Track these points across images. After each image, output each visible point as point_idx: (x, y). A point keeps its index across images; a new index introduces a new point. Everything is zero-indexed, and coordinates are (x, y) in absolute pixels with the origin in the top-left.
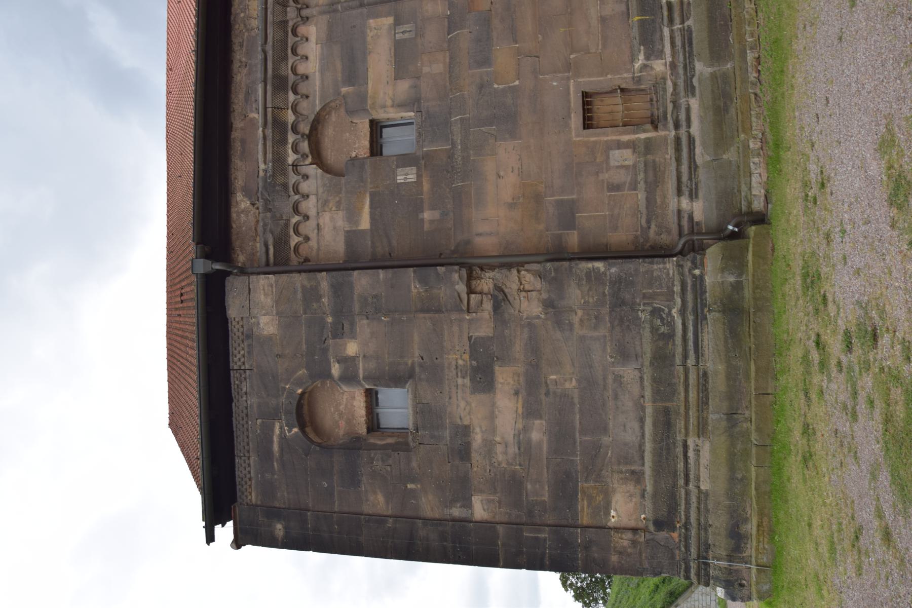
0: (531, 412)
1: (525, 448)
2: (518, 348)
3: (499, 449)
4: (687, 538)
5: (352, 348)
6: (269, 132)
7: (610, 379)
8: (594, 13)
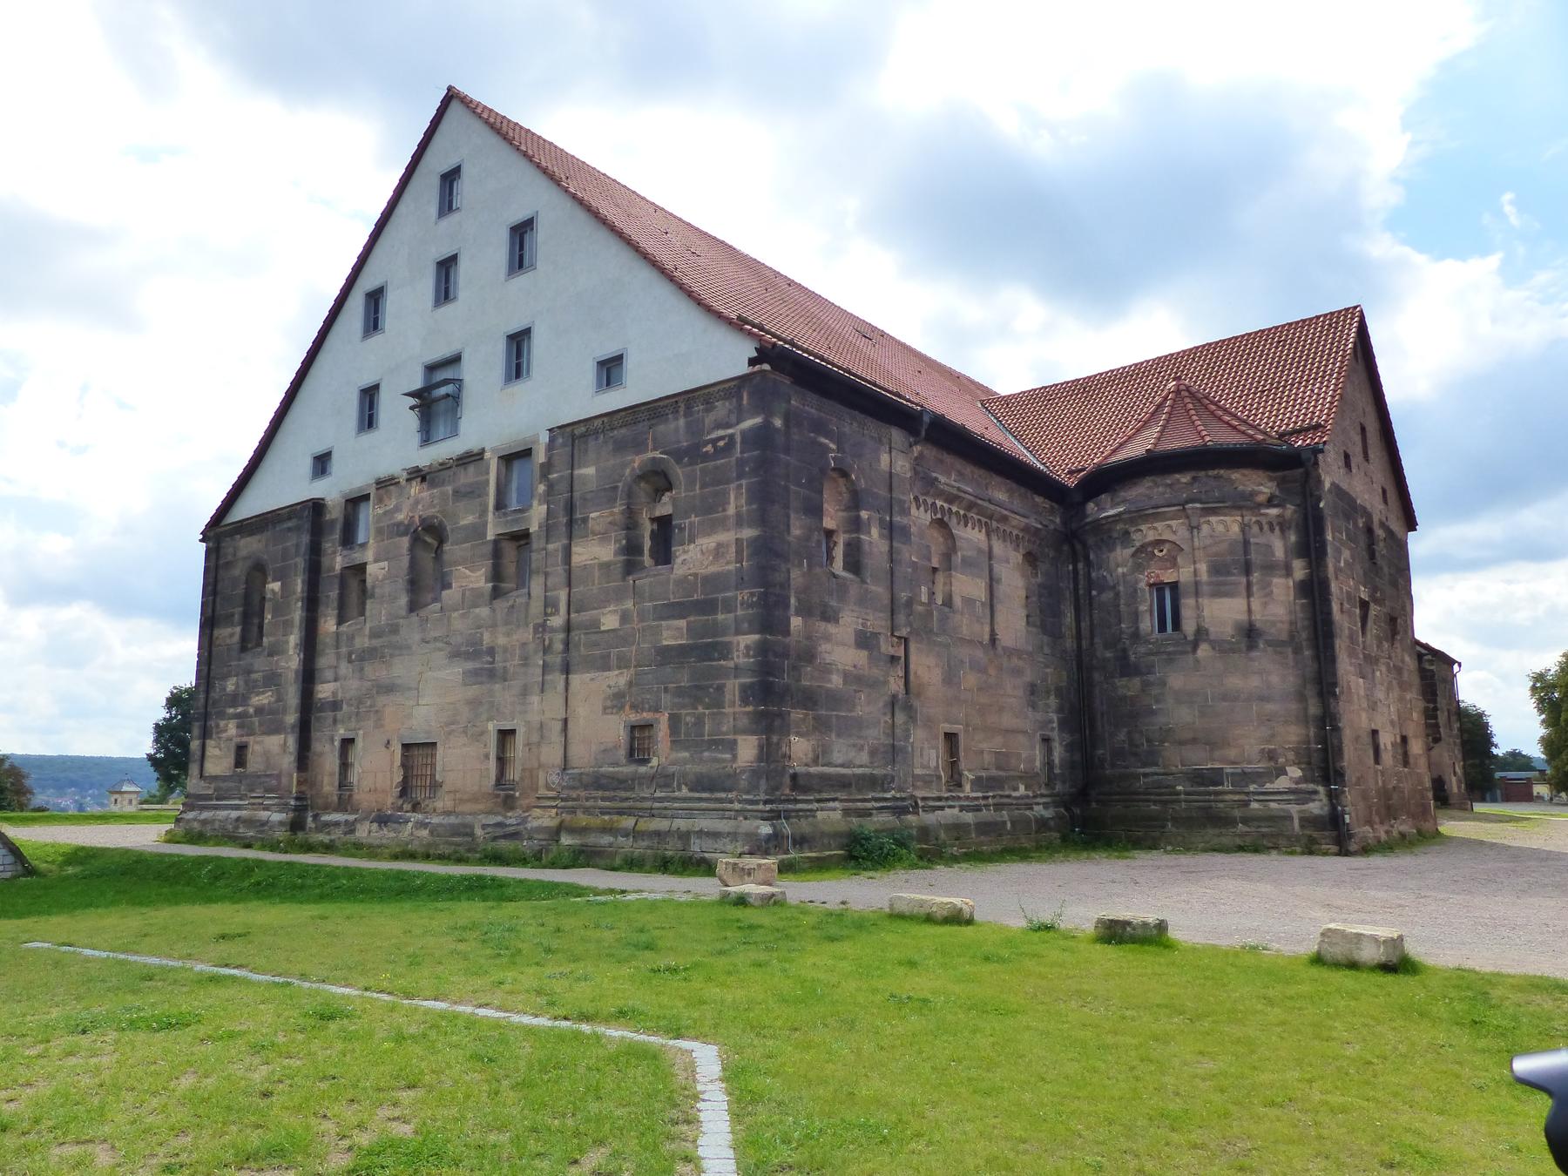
0: (846, 676)
1: (826, 669)
2: (876, 672)
4: (788, 801)
5: (875, 532)
6: (955, 492)
7: (862, 742)
8: (984, 746)
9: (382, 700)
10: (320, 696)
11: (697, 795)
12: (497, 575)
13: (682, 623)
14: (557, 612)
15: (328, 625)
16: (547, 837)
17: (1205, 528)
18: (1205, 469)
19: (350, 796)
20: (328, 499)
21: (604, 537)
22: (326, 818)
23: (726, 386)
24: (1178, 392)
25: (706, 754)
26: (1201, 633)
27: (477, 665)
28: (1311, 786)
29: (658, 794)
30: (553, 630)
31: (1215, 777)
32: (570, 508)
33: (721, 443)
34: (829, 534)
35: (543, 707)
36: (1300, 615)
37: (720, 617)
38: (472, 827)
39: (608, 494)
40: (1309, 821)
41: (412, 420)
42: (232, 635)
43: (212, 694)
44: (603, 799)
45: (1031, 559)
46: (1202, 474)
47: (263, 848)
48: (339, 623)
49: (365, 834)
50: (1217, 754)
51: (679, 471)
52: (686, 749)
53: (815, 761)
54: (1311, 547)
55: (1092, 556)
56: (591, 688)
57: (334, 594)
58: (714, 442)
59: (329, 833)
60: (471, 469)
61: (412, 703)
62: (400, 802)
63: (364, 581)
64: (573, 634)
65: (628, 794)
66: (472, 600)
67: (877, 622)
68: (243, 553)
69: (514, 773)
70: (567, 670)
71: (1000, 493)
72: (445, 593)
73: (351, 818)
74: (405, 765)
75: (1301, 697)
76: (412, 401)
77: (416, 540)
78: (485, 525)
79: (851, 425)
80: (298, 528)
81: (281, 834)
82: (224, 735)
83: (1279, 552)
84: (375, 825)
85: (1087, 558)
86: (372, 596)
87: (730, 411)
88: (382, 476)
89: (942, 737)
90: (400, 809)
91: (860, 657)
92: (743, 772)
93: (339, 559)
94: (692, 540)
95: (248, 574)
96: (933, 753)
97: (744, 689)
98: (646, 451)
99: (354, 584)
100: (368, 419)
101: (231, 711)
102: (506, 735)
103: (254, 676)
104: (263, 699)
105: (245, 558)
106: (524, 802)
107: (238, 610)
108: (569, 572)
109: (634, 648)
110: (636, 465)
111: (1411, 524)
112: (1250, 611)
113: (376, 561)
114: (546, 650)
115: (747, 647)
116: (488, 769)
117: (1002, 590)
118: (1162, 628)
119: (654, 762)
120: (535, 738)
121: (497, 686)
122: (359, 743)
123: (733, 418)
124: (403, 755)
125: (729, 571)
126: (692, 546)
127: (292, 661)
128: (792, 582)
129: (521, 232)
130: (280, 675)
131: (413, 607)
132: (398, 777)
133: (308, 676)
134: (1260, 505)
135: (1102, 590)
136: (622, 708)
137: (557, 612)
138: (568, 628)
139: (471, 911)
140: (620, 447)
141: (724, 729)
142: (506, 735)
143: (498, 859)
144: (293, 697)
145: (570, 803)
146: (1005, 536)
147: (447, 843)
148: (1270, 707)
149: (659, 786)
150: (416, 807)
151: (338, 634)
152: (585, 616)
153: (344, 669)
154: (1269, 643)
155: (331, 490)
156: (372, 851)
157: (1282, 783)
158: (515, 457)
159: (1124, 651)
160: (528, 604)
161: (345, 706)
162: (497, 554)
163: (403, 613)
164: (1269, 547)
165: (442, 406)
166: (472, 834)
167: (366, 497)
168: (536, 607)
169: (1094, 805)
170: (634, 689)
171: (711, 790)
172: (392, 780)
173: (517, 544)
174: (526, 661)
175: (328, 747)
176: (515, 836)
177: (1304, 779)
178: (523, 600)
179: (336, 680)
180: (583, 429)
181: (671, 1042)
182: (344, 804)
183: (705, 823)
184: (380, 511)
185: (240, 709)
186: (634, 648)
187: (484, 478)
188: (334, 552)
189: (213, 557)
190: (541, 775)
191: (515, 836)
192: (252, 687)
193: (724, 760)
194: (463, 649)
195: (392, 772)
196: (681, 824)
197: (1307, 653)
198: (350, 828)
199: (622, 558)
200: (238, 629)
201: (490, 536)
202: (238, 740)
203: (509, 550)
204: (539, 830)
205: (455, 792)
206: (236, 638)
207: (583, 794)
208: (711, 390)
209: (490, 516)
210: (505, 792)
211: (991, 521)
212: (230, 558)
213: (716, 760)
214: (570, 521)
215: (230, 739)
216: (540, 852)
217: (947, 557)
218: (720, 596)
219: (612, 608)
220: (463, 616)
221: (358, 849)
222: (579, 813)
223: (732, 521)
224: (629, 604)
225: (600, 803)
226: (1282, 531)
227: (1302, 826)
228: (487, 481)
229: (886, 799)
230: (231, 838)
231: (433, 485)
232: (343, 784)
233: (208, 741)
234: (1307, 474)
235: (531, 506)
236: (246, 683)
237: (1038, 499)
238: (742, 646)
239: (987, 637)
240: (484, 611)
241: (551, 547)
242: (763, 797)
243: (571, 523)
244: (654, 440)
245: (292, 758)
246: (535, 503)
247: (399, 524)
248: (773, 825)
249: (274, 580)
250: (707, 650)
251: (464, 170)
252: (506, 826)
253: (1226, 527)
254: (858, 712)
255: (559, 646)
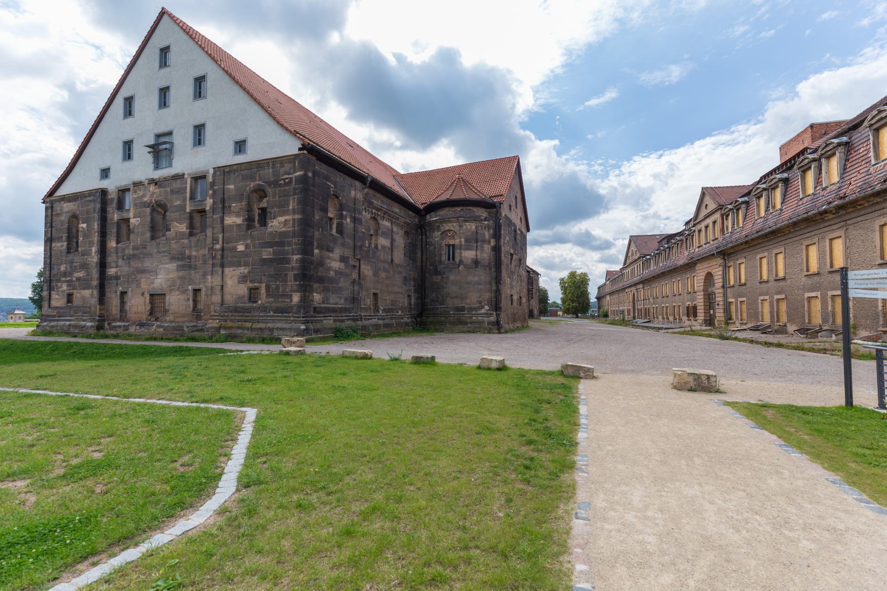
0: (336, 272)
1: (329, 269)
3: (329, 261)
4: (312, 317)
5: (348, 220)
8: (387, 298)
9: (139, 276)
10: (109, 273)
11: (277, 315)
12: (191, 226)
13: (271, 250)
14: (218, 243)
15: (112, 244)
16: (214, 330)
17: (464, 226)
18: (465, 206)
19: (126, 315)
20: (109, 189)
21: (238, 215)
22: (114, 324)
23: (289, 158)
24: (459, 179)
25: (280, 299)
26: (461, 262)
27: (184, 263)
28: (492, 312)
29: (261, 314)
30: (216, 250)
31: (462, 309)
32: (223, 201)
33: (287, 181)
34: (331, 219)
35: (213, 281)
36: (492, 257)
37: (286, 248)
38: (183, 327)
39: (239, 197)
40: (490, 323)
41: (150, 158)
42: (62, 246)
43: (53, 272)
44: (238, 316)
45: (407, 233)
46: (464, 208)
47: (83, 337)
48: (117, 243)
49: (133, 331)
50: (464, 301)
51: (270, 190)
52: (272, 297)
53: (323, 302)
54: (497, 236)
55: (427, 234)
56: (232, 275)
57: (114, 230)
58: (284, 180)
59: (116, 330)
60: (179, 181)
61: (153, 277)
62: (150, 317)
63: (129, 226)
64: (225, 252)
65: (249, 314)
66: (180, 236)
67: (348, 253)
68: (66, 210)
69: (200, 306)
70: (223, 266)
71: (396, 209)
72: (168, 233)
73: (126, 324)
74: (151, 303)
75: (490, 284)
76: (150, 150)
77: (153, 210)
78: (185, 205)
79: (340, 178)
80: (94, 201)
81: (93, 331)
82: (61, 289)
83: (487, 237)
84: (138, 327)
85: (426, 234)
86: (133, 232)
87: (291, 168)
88: (136, 181)
89: (372, 295)
90: (150, 320)
91: (342, 265)
92: (295, 306)
93: (116, 216)
94: (275, 218)
95: (69, 219)
96: (369, 300)
97: (295, 275)
98: (256, 181)
99: (124, 227)
100: (128, 155)
101: (64, 279)
102: (196, 291)
103: (74, 264)
104: (81, 274)
105: (67, 212)
106: (206, 317)
107: (65, 236)
108: (223, 227)
109: (251, 259)
110: (252, 186)
111: (528, 230)
112: (476, 255)
113: (134, 217)
114: (214, 258)
115: (297, 260)
116: (189, 305)
117: (396, 243)
118: (449, 259)
119: (260, 302)
120: (209, 292)
121: (192, 272)
122: (129, 294)
123: (292, 171)
124: (150, 299)
125: (290, 231)
126: (275, 220)
127: (94, 258)
128: (315, 237)
129: (200, 81)
130: (88, 264)
131: (153, 238)
132: (148, 308)
133: (103, 265)
134: (482, 220)
135: (430, 246)
136: (246, 281)
137: (218, 243)
138: (223, 249)
139: (172, 360)
140: (244, 178)
141: (288, 290)
142: (196, 291)
143: (193, 339)
144: (95, 273)
145: (225, 318)
146: (398, 225)
147: (171, 333)
148: (480, 286)
149: (261, 311)
150: (157, 320)
151: (117, 248)
152: (230, 245)
153: (120, 262)
154: (482, 266)
155: (111, 185)
156: (137, 338)
157: (483, 311)
158: (198, 178)
159: (436, 266)
160: (205, 239)
161: (122, 278)
162: (191, 218)
163: (148, 240)
164: (484, 234)
165: (164, 153)
166: (183, 330)
167: (129, 190)
168: (209, 241)
169: (424, 318)
170: (251, 274)
171: (282, 312)
172: (145, 308)
173: (200, 215)
174: (205, 262)
175: (114, 295)
176: (202, 330)
177: (489, 310)
178: (204, 237)
179: (117, 267)
180: (229, 169)
181: (239, 409)
182: (122, 319)
183: (279, 325)
184: (136, 196)
185: (68, 279)
186: (251, 259)
187: (185, 186)
188: (114, 213)
189: (50, 211)
190: (212, 307)
191: (202, 330)
192: (74, 269)
193: (287, 302)
194: (177, 256)
195: (145, 305)
196: (270, 325)
197: (493, 270)
198: (126, 328)
199: (246, 223)
200: (65, 244)
201: (188, 210)
202: (68, 291)
203: (197, 218)
204: (212, 328)
205: (174, 313)
206: (65, 247)
207: (230, 314)
208: (283, 159)
209: (188, 202)
210: (196, 313)
211: (392, 218)
212: (59, 212)
213: (283, 302)
214: (223, 206)
215: (64, 291)
216: (212, 336)
217: (377, 231)
218: (286, 240)
219: (242, 242)
220: (176, 243)
221: (130, 336)
222: (228, 321)
223: (291, 211)
224: (249, 241)
225: (237, 318)
226: (488, 229)
227: (488, 325)
228: (186, 187)
229: (350, 316)
230: (67, 333)
231: (160, 187)
232: (122, 309)
233: (52, 292)
234: (497, 211)
235: (206, 199)
236: (71, 267)
237: (410, 213)
238: (295, 259)
239: (390, 260)
240: (186, 241)
241: (215, 216)
242: (302, 315)
243: (223, 207)
244: (259, 177)
245: (96, 300)
246: (208, 198)
247: (145, 202)
248: (306, 326)
249: (83, 223)
250: (280, 260)
251: (171, 48)
252: (197, 326)
253: (472, 226)
254: (341, 285)
255: (219, 257)
